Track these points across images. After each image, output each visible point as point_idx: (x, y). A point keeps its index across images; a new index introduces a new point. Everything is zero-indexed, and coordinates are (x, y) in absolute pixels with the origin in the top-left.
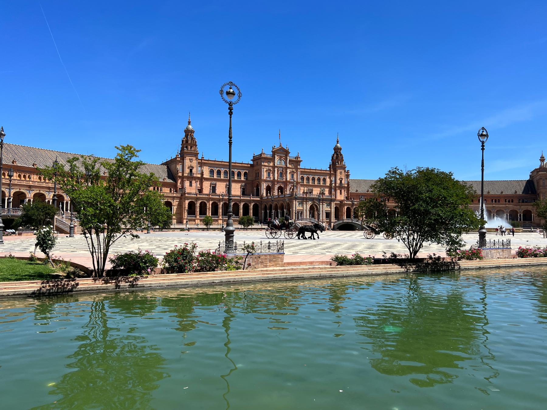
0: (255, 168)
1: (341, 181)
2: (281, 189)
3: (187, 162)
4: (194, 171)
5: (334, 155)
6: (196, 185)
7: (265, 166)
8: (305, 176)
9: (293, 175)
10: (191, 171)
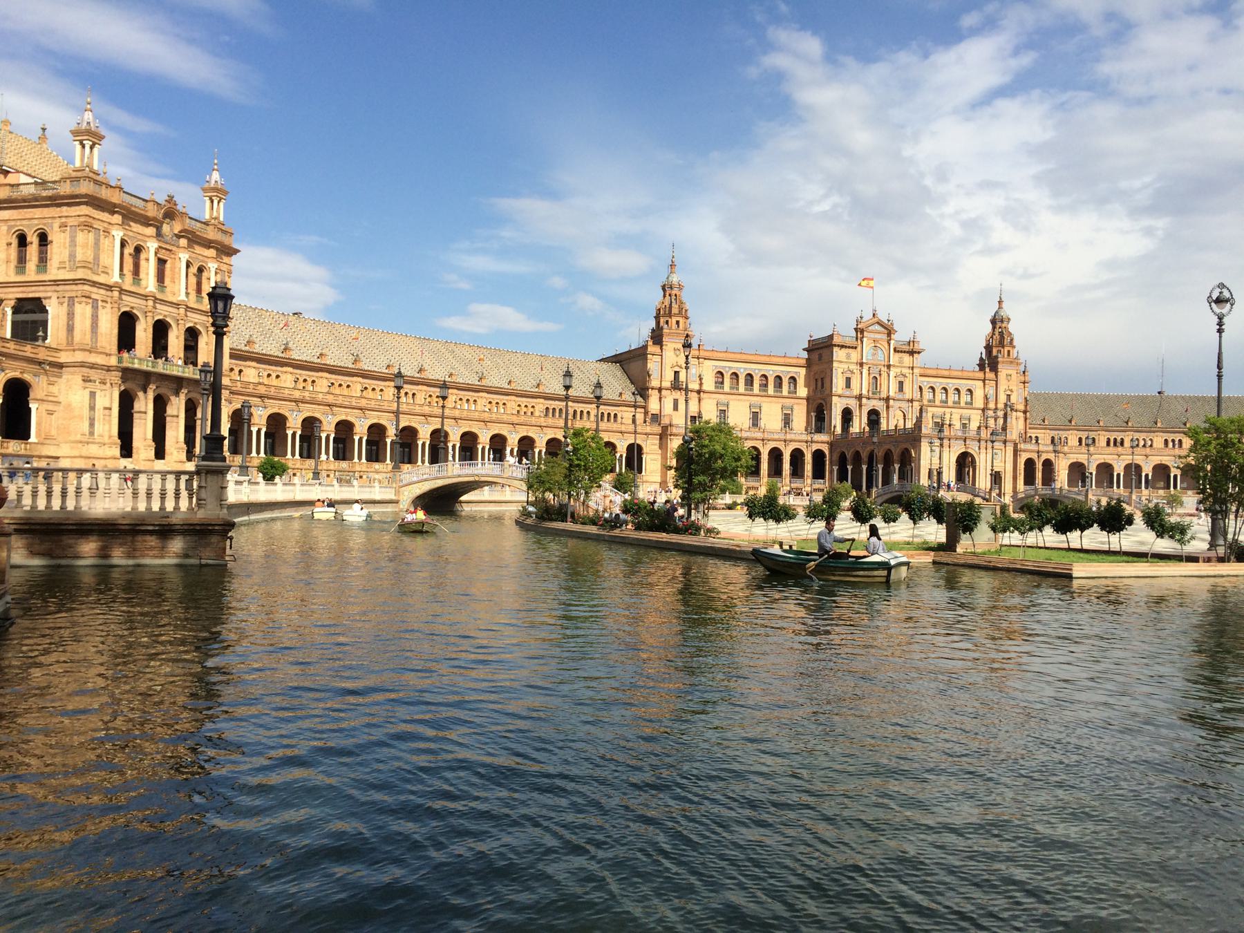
9: (901, 383)
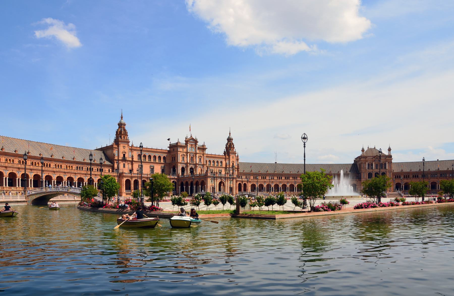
0: (172, 154)
1: (233, 164)
2: (192, 170)
5: (227, 144)
6: (128, 166)
7: (180, 152)
9: (200, 159)
10: (124, 155)
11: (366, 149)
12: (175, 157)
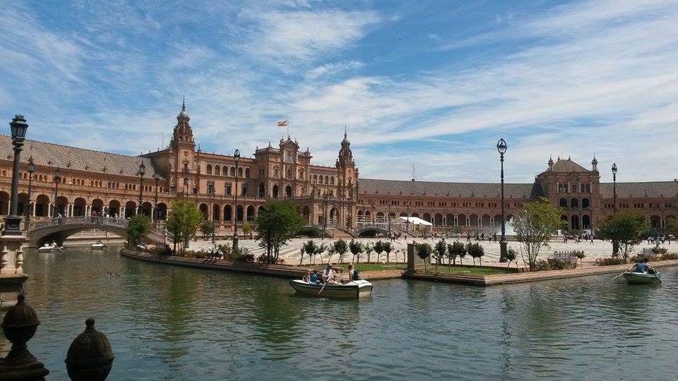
2: (289, 190)
3: (182, 156)
4: (190, 166)
5: (341, 151)
7: (272, 162)
8: (313, 175)
10: (186, 165)
11: (555, 161)
12: (263, 170)
